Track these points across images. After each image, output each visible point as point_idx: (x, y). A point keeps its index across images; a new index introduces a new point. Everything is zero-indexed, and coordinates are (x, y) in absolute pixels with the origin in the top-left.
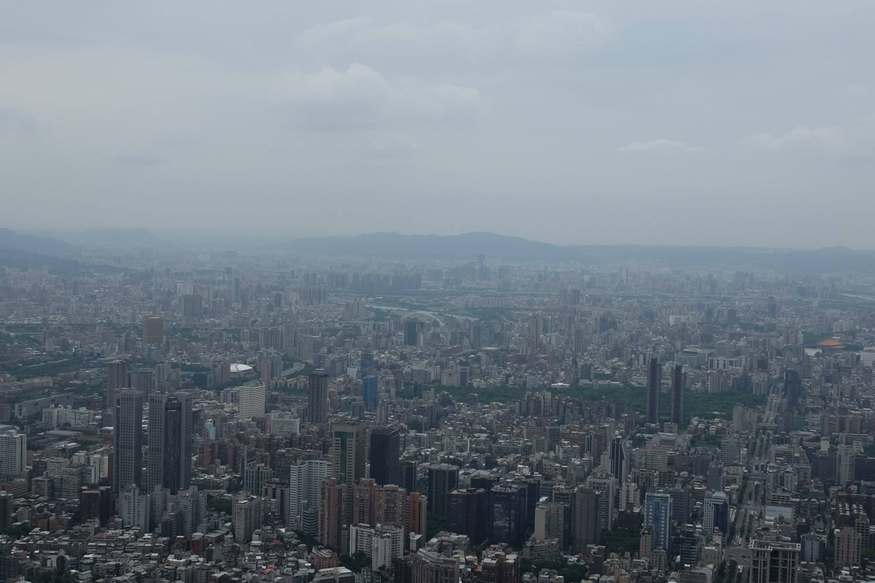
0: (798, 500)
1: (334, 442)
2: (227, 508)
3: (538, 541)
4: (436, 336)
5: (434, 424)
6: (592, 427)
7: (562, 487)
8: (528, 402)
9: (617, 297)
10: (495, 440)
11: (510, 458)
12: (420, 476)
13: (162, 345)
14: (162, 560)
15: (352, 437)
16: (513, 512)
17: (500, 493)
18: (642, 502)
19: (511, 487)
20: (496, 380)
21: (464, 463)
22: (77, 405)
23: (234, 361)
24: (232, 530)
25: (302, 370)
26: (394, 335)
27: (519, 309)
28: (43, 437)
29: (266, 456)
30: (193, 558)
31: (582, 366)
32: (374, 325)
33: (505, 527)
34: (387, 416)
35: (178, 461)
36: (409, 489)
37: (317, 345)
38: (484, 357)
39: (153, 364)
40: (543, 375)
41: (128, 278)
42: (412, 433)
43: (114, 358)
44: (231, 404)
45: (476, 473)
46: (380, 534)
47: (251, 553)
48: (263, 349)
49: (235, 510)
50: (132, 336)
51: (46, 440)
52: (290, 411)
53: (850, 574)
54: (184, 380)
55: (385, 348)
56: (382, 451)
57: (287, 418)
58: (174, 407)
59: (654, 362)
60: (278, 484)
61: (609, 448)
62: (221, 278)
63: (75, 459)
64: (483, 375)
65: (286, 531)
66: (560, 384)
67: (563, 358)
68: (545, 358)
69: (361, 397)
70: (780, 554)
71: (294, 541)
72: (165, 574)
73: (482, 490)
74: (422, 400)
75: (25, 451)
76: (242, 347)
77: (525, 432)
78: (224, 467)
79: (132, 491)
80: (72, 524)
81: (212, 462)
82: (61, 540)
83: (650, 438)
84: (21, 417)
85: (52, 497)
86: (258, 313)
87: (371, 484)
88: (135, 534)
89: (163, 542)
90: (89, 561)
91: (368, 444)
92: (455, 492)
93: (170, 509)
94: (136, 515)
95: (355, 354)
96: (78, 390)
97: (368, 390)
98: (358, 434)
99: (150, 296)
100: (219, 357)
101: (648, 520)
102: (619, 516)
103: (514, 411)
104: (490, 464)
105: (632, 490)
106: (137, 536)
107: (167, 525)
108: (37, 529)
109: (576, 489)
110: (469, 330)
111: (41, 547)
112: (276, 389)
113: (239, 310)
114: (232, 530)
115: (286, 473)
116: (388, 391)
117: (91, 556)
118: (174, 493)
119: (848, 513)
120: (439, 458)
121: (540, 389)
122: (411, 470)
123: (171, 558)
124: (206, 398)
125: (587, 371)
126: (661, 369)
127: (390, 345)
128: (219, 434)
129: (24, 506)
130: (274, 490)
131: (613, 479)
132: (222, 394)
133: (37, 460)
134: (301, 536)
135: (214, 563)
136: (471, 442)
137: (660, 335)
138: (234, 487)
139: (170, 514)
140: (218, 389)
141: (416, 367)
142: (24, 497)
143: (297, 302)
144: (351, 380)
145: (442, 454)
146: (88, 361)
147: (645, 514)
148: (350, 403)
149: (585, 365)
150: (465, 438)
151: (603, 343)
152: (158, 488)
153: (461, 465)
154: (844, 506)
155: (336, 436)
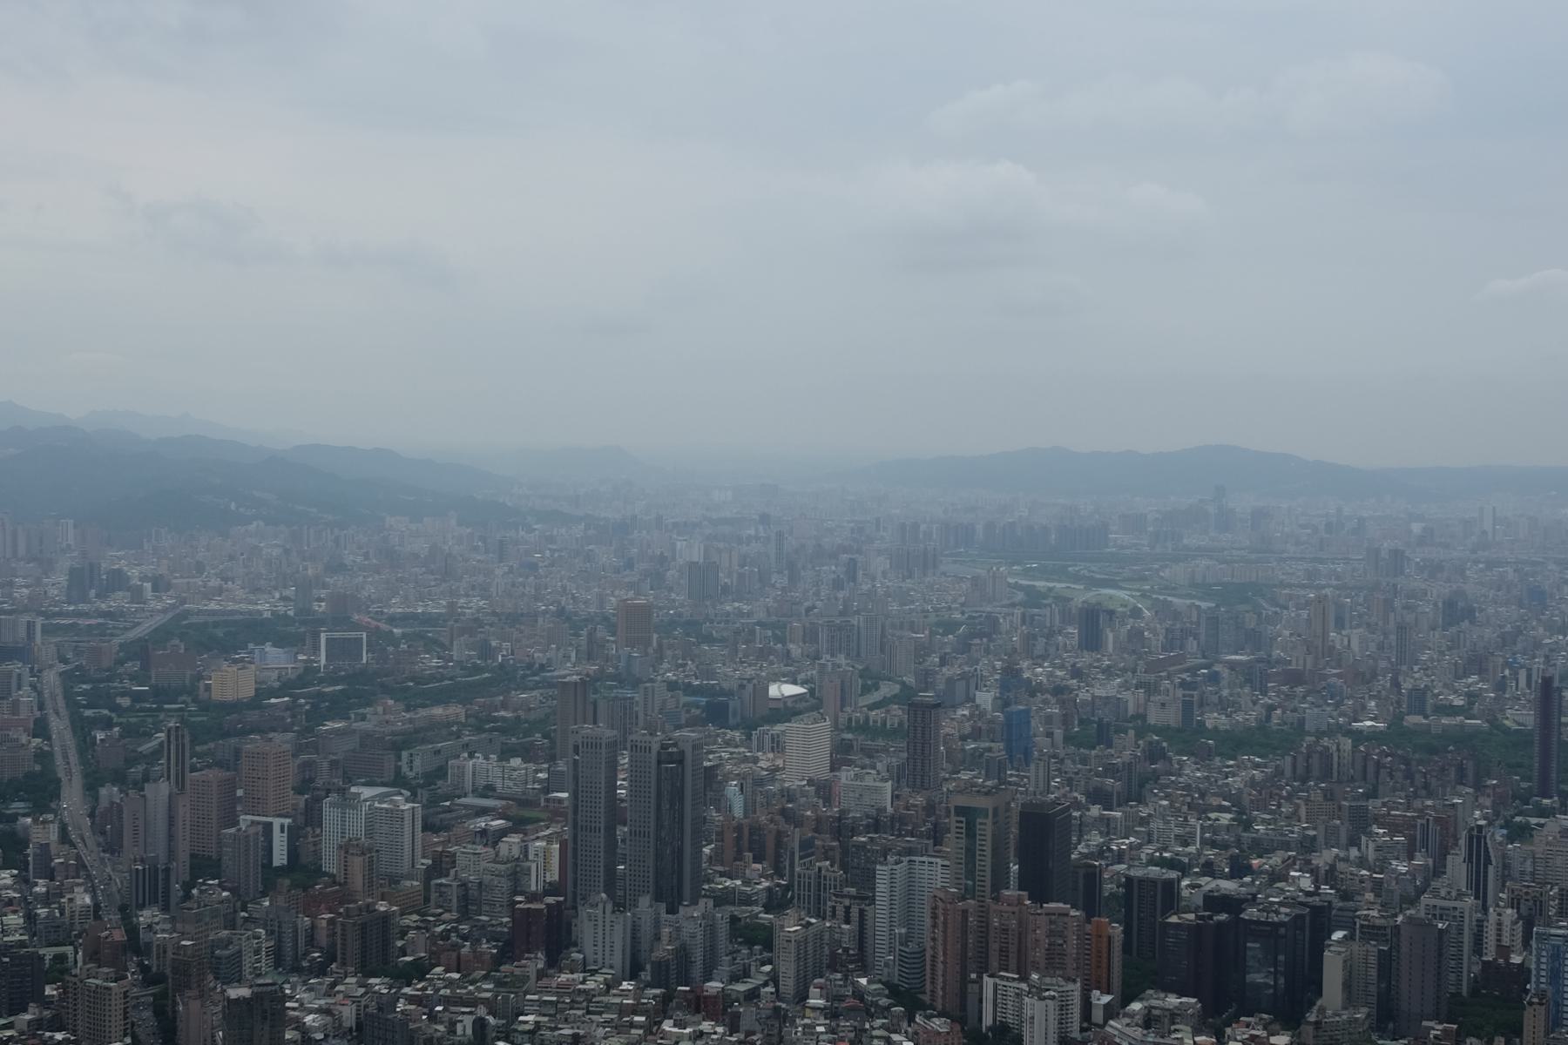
1: (954, 825)
2: (762, 939)
3: (1329, 1012)
4: (1136, 635)
5: (1135, 793)
6: (1429, 803)
7: (1375, 913)
8: (1309, 756)
9: (1476, 562)
10: (1247, 826)
11: (1276, 859)
12: (1109, 888)
13: (650, 651)
14: (652, 1027)
15: (986, 816)
16: (1281, 958)
17: (1258, 923)
18: (1526, 944)
19: (1277, 913)
20: (1248, 717)
21: (1190, 866)
22: (506, 754)
23: (776, 678)
24: (774, 978)
25: (895, 696)
26: (1060, 632)
27: (1290, 586)
28: (449, 810)
29: (832, 848)
31: (1410, 691)
32: (1023, 615)
33: (1267, 985)
34: (1049, 779)
35: (679, 853)
36: (1091, 910)
37: (922, 651)
38: (1225, 673)
39: (636, 683)
40: (1337, 705)
41: (591, 532)
42: (1095, 811)
43: (569, 672)
44: (771, 755)
45: (1213, 885)
46: (1038, 992)
47: (807, 1021)
50: (599, 635)
51: (454, 815)
52: (874, 768)
54: (688, 711)
55: (1044, 657)
56: (1040, 842)
57: (869, 781)
58: (672, 760)
59: (1547, 682)
61: (1462, 842)
62: (752, 532)
63: (503, 848)
64: (1223, 706)
66: (1369, 723)
67: (1374, 675)
68: (1338, 676)
69: (1001, 745)
71: (884, 1002)
73: (1223, 917)
74: (1112, 751)
75: (419, 834)
76: (788, 652)
77: (1303, 812)
78: (759, 866)
80: (498, 961)
81: (739, 857)
82: (480, 990)
83: (1542, 826)
84: (411, 774)
85: (465, 915)
86: (817, 594)
87: (1020, 902)
88: (606, 982)
89: (654, 997)
90: (527, 1027)
91: (1015, 830)
92: (1174, 919)
93: (665, 939)
94: (607, 949)
95: (990, 666)
96: (507, 728)
97: (1014, 733)
98: (995, 810)
99: (630, 565)
100: (750, 672)
101: (1538, 976)
102: (1483, 970)
103: (1282, 773)
105: (1507, 921)
106: (609, 986)
107: (660, 968)
108: (439, 969)
109: (1400, 919)
110: (1198, 624)
111: (446, 1001)
112: (849, 729)
113: (783, 589)
114: (774, 978)
115: (869, 879)
116: (1050, 735)
117: (530, 1018)
118: (672, 910)
120: (1143, 856)
121: (1331, 732)
123: (667, 1026)
124: (728, 743)
125: (1418, 699)
126: (1561, 698)
127: (1052, 650)
128: (749, 808)
129: (418, 928)
130: (847, 909)
131: (1470, 900)
132: (754, 737)
133: (440, 849)
136: (1202, 827)
137: (1559, 633)
138: (776, 903)
139: (665, 949)
140: (748, 727)
141: (1100, 692)
142: (417, 912)
143: (884, 574)
144: (982, 714)
145: (1149, 849)
146: (524, 677)
147: (1533, 966)
148: (981, 755)
149: (1415, 689)
150: (1192, 821)
151: (1450, 649)
152: (645, 901)
153: (1185, 870)
155: (957, 814)
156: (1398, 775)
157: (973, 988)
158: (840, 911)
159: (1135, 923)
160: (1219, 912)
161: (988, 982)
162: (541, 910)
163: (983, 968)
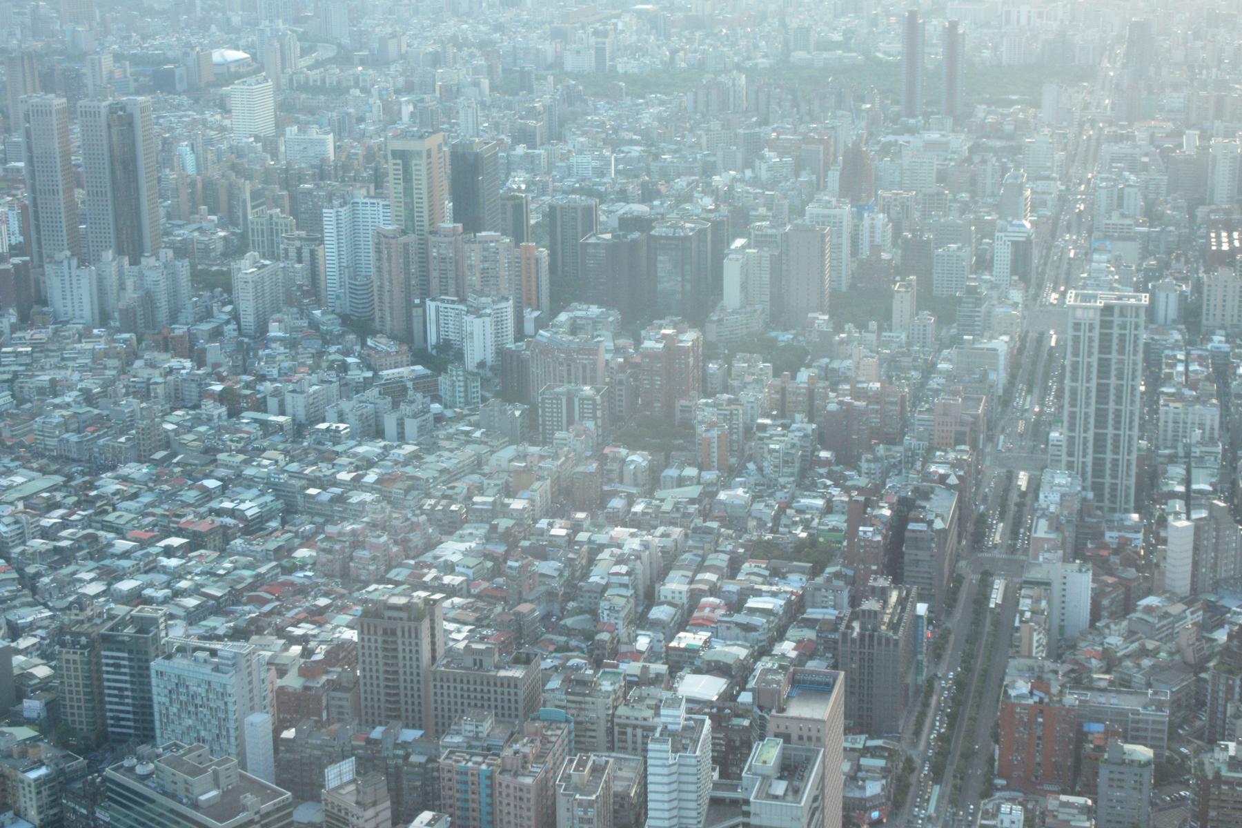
0: (1145, 229)
2: (223, 284)
10: (656, 157)
11: (681, 183)
17: (667, 238)
23: (217, 45)
29: (282, 197)
30: (174, 363)
42: (521, 149)
46: (476, 312)
48: (264, 24)
49: (238, 285)
53: (1227, 342)
60: (306, 240)
65: (323, 314)
70: (1116, 312)
72: (131, 390)
73: (636, 235)
77: (704, 141)
78: (214, 218)
79: (66, 262)
81: (194, 210)
92: (593, 240)
104: (648, 195)
109: (788, 227)
114: (235, 316)
118: (135, 262)
119: (1225, 247)
122: (518, 208)
130: (299, 250)
134: (345, 319)
135: (209, 369)
136: (616, 160)
138: (235, 249)
139: (131, 295)
153: (602, 197)
154: (1218, 237)
155: (394, 158)
156: (787, 104)
157: (417, 312)
158: (292, 253)
159: (559, 246)
160: (632, 231)
161: (431, 305)
162: (8, 270)
163: (425, 294)
